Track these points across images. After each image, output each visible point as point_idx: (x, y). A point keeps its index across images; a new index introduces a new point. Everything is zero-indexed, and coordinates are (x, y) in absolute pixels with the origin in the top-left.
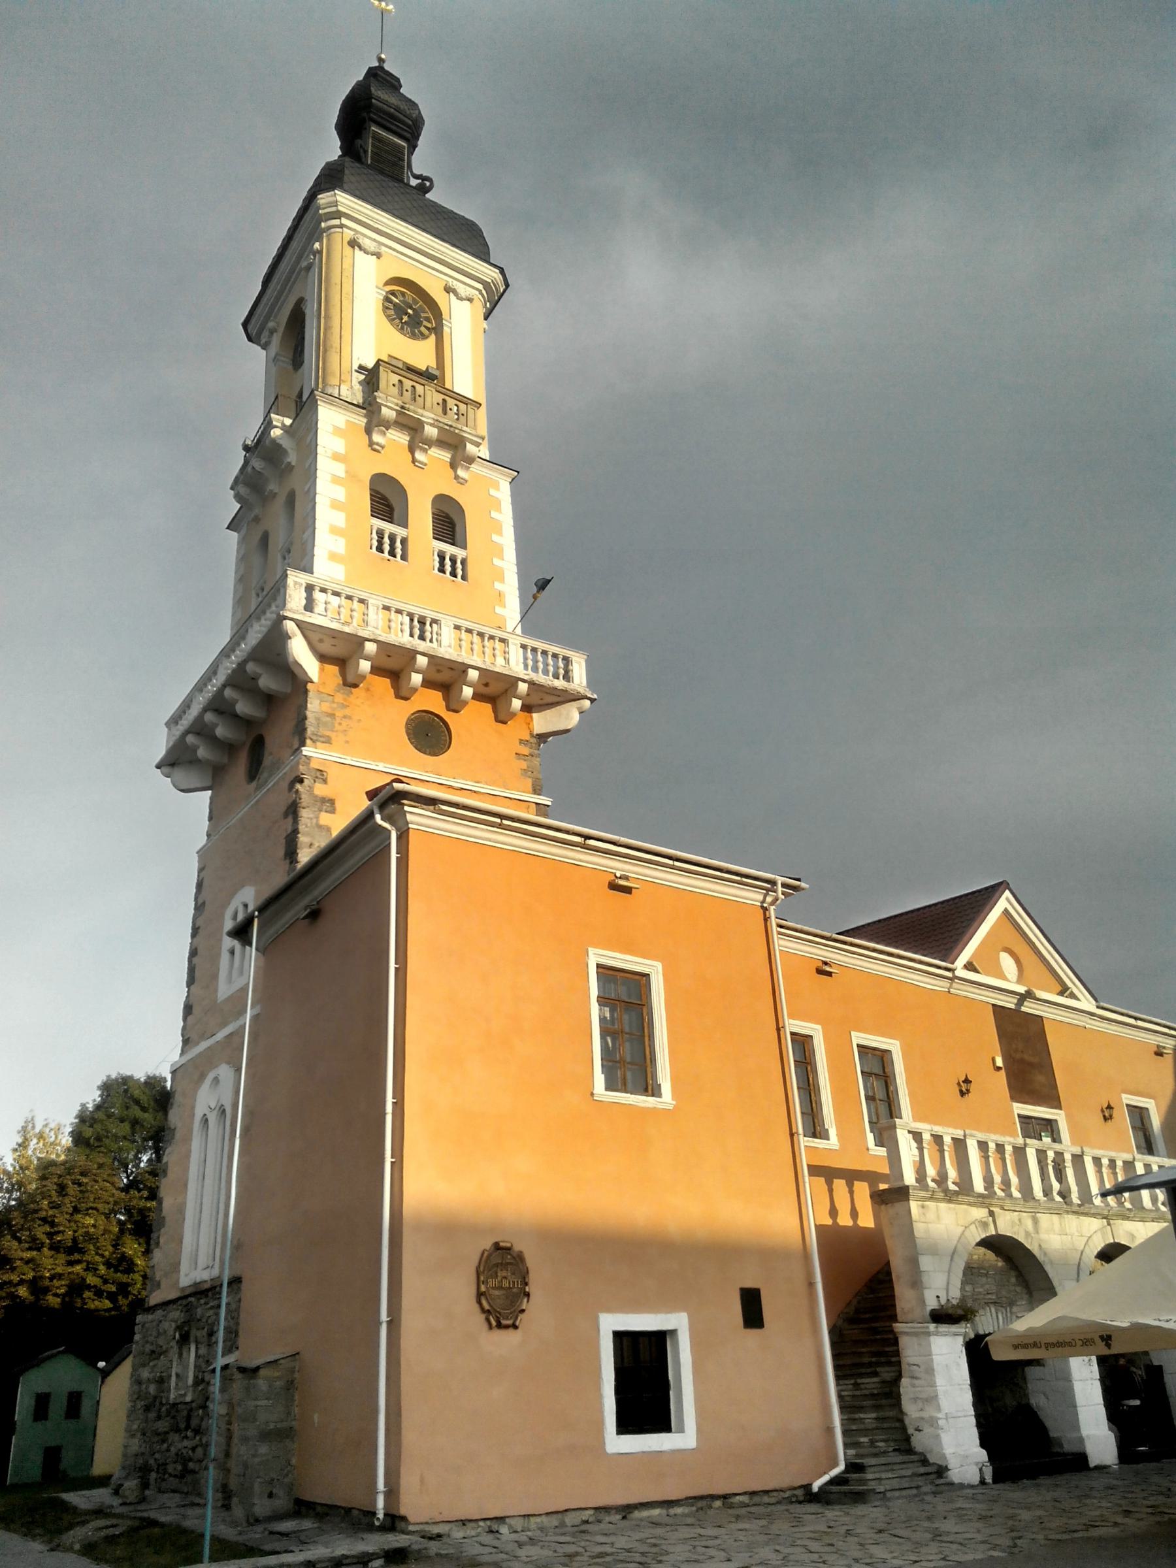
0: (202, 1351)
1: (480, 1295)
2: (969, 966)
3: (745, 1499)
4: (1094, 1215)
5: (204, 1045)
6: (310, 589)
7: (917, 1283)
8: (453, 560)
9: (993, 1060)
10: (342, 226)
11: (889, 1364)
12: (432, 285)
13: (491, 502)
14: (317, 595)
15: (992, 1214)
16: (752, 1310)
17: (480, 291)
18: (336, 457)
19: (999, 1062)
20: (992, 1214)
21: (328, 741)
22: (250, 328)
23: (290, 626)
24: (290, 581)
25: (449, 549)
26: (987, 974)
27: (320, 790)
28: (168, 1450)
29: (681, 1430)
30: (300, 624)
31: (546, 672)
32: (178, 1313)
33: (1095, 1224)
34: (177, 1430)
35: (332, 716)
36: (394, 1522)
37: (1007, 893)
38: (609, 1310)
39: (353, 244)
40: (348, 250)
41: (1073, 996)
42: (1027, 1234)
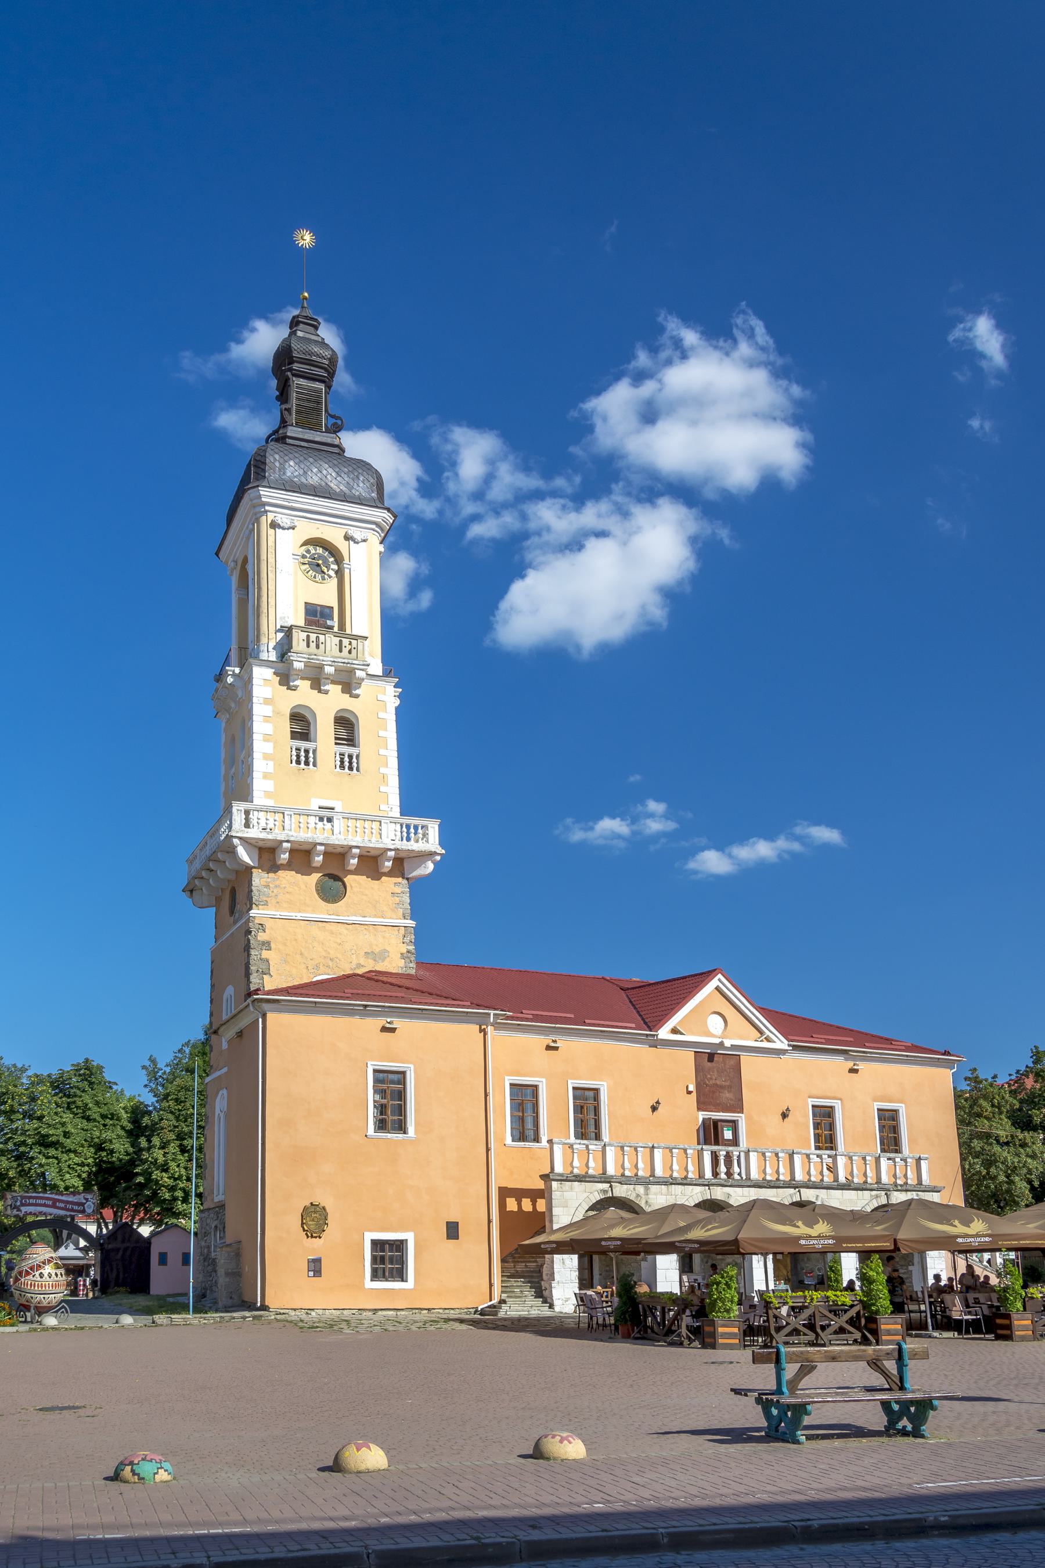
1: (302, 1223)
2: (674, 1031)
3: (441, 1311)
6: (247, 813)
7: (551, 1221)
14: (254, 816)
15: (611, 1186)
16: (453, 1231)
19: (691, 1088)
20: (611, 1186)
23: (236, 841)
24: (234, 810)
26: (693, 1034)
30: (240, 838)
35: (267, 886)
36: (264, 1308)
37: (720, 976)
38: (370, 1231)
41: (768, 1040)
42: (638, 1196)
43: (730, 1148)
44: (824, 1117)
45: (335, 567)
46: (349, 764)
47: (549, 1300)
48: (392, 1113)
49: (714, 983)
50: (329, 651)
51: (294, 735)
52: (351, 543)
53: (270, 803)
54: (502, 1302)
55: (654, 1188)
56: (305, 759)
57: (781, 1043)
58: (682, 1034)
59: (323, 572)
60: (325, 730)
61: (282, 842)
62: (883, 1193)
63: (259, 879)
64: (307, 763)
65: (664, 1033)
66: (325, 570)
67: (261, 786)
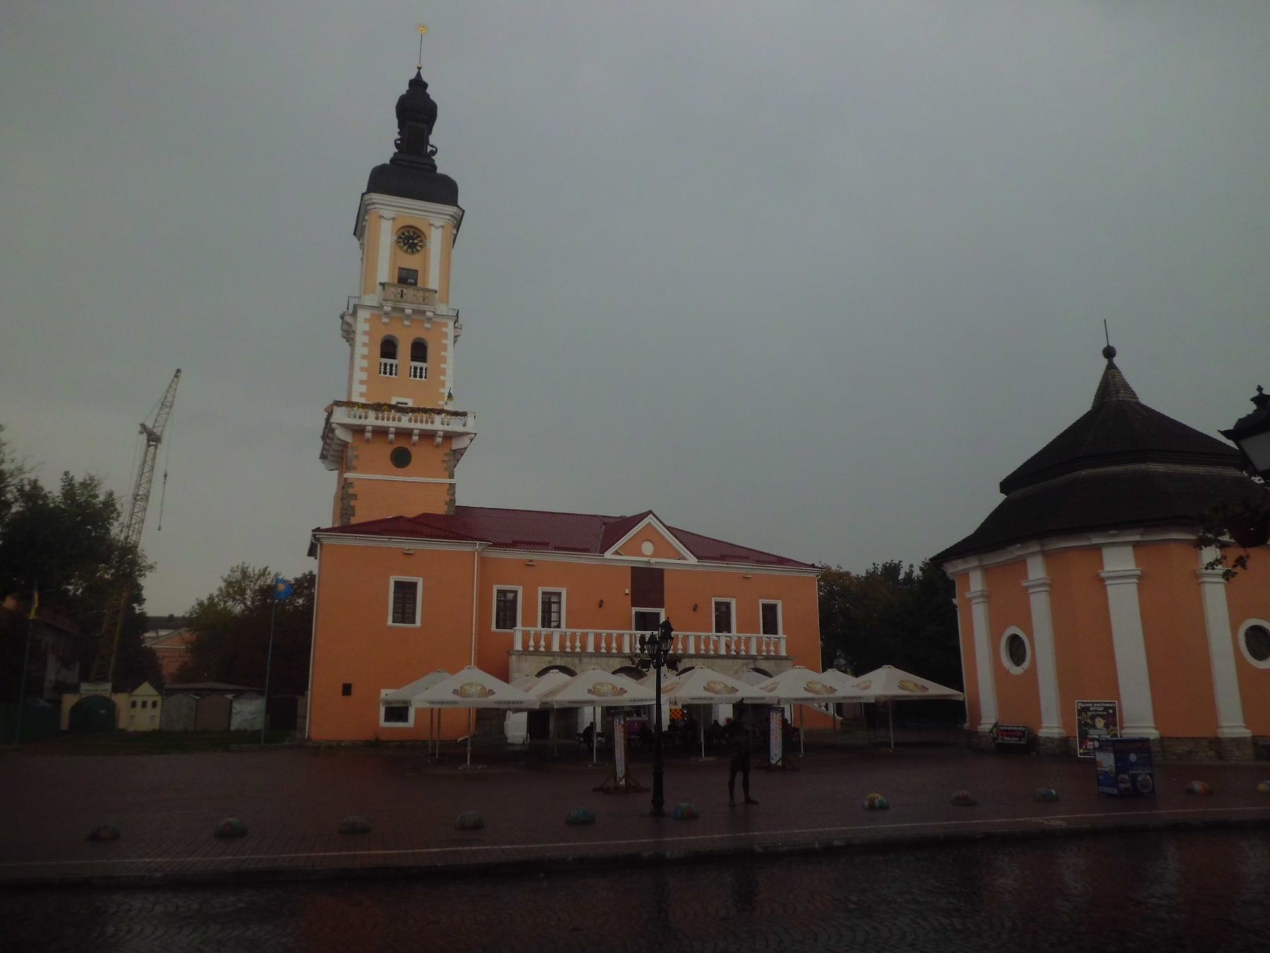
2: (617, 553)
18: (365, 333)
19: (627, 591)
21: (354, 469)
27: (351, 491)
33: (618, 660)
41: (684, 559)
48: (405, 608)
51: (384, 355)
53: (363, 400)
55: (586, 660)
57: (692, 560)
60: (404, 350)
65: (608, 555)
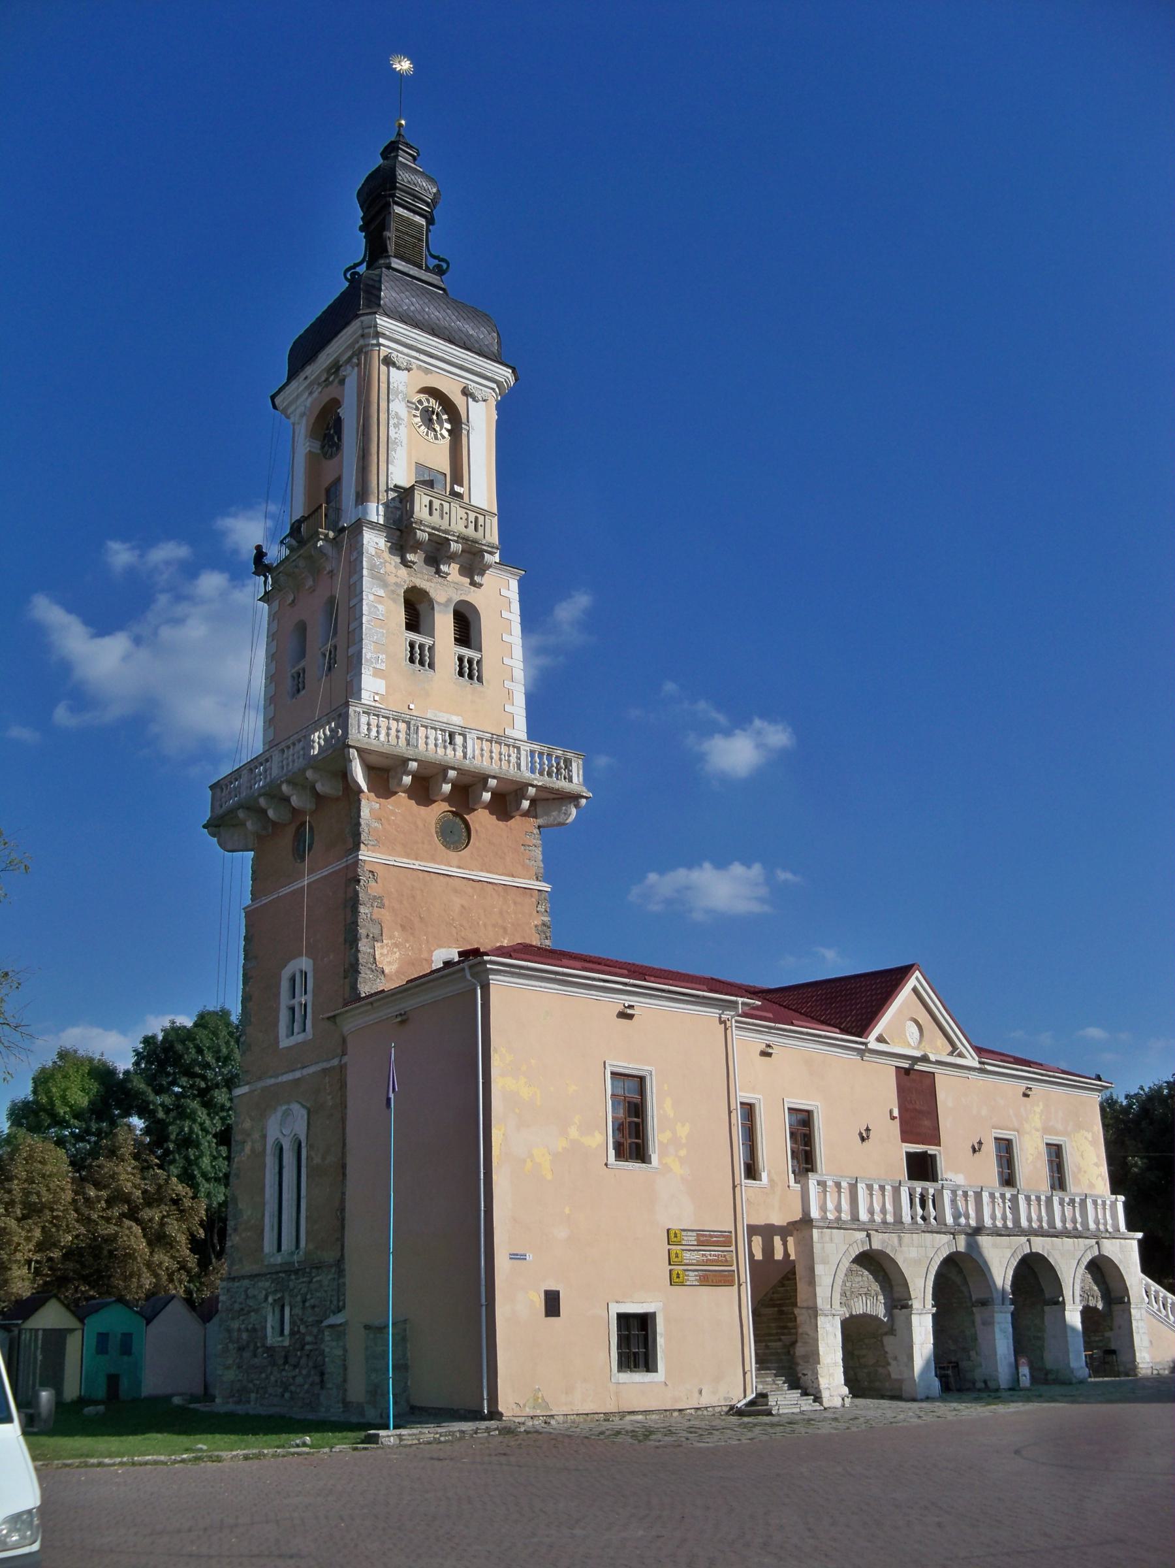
0: (298, 1311)
4: (944, 1233)
5: (272, 1081)
7: (812, 1281)
8: (470, 661)
9: (891, 1112)
10: (379, 345)
11: (790, 1334)
12: (452, 390)
13: (499, 596)
17: (493, 389)
19: (896, 1113)
20: (868, 1236)
22: (278, 400)
24: (351, 709)
25: (467, 652)
28: (267, 1378)
29: (656, 1371)
30: (358, 749)
31: (550, 774)
32: (268, 1284)
33: (946, 1238)
34: (274, 1364)
36: (495, 1415)
39: (388, 362)
40: (383, 368)
41: (961, 1055)
42: (893, 1248)
43: (927, 1184)
44: (1006, 1149)
45: (448, 426)
46: (469, 671)
47: (810, 1391)
49: (912, 983)
50: (456, 522)
52: (470, 400)
54: (763, 1396)
55: (906, 1237)
56: (420, 657)
57: (972, 1060)
58: (887, 1043)
59: (435, 430)
61: (405, 761)
62: (1094, 1241)
63: (369, 807)
64: (422, 663)
65: (872, 1041)
66: (437, 428)
67: (372, 686)
